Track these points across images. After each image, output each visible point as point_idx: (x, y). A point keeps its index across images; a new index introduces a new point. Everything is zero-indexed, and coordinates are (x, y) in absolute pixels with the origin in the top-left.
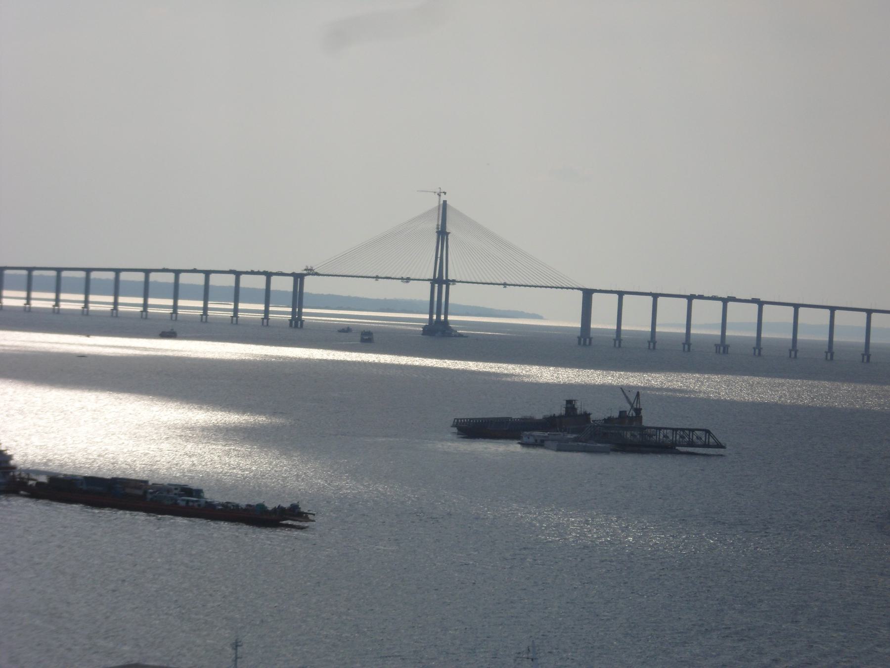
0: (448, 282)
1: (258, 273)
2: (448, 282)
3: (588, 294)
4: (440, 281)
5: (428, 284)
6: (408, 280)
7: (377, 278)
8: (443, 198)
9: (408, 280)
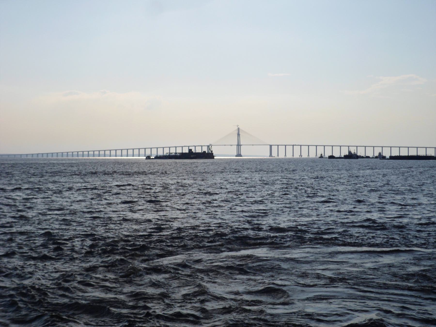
0: (240, 145)
1: (200, 146)
2: (240, 145)
3: (271, 146)
4: (239, 145)
5: (236, 146)
6: (232, 145)
7: (225, 145)
8: (238, 127)
9: (232, 145)
